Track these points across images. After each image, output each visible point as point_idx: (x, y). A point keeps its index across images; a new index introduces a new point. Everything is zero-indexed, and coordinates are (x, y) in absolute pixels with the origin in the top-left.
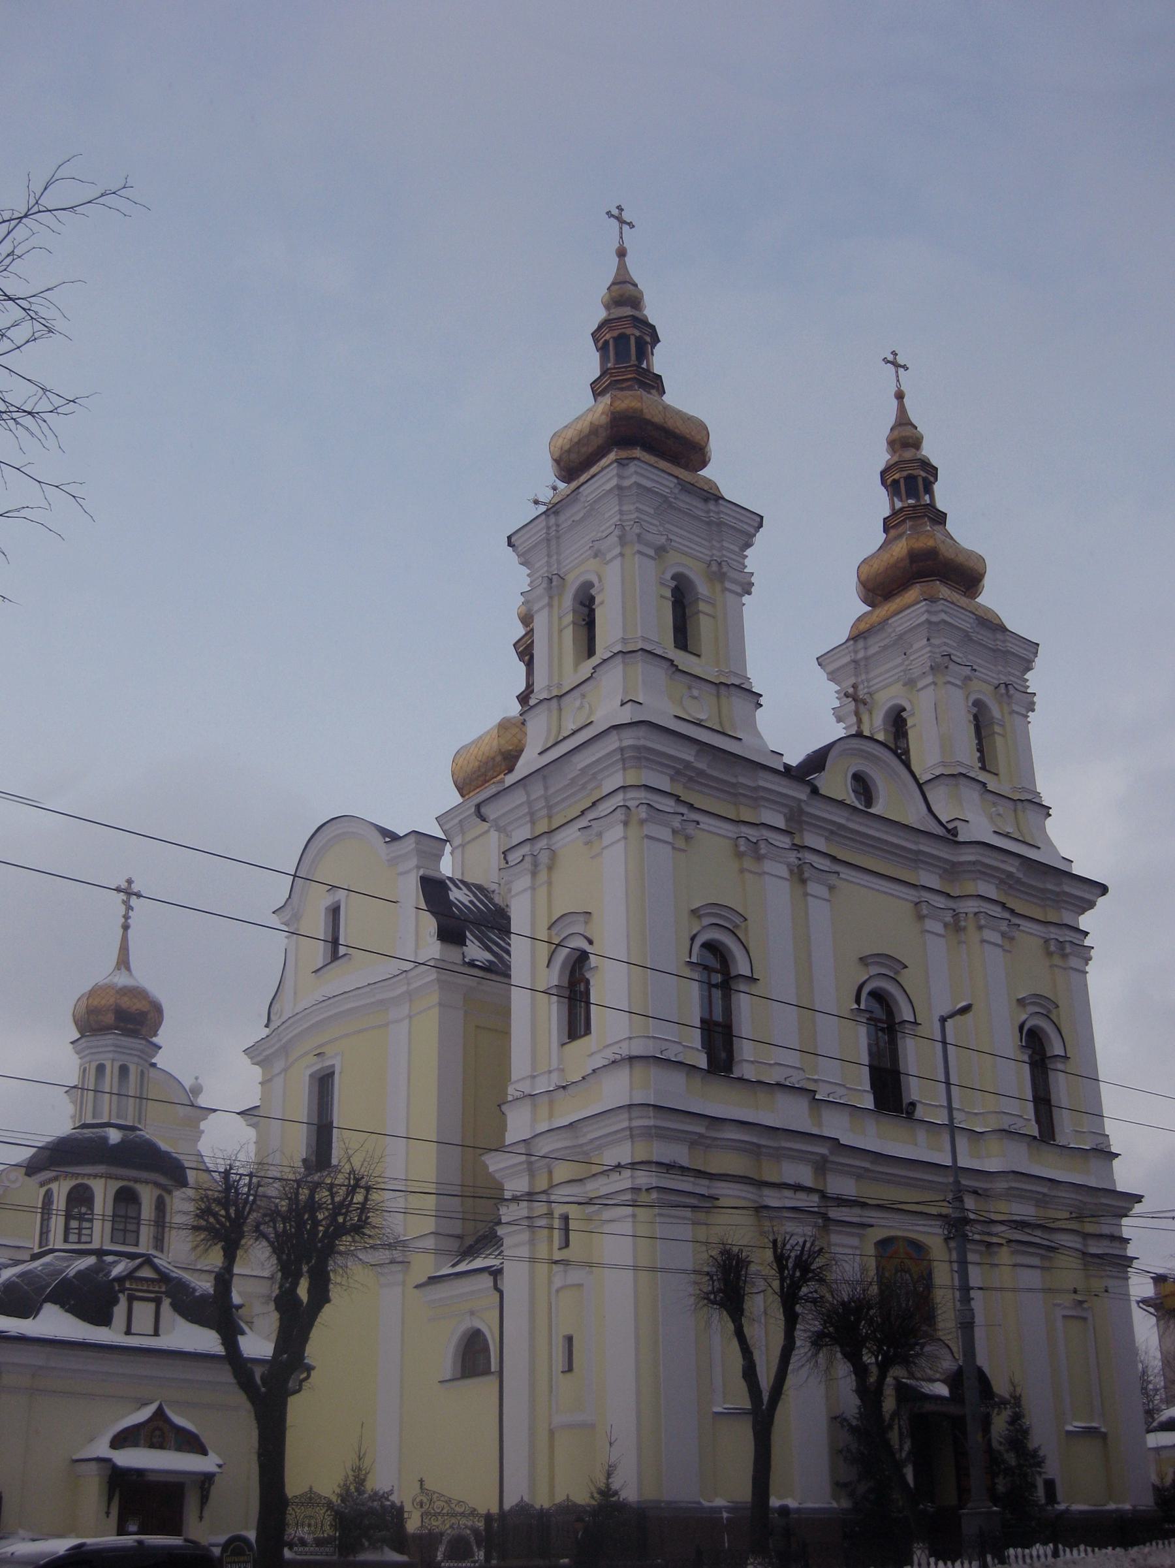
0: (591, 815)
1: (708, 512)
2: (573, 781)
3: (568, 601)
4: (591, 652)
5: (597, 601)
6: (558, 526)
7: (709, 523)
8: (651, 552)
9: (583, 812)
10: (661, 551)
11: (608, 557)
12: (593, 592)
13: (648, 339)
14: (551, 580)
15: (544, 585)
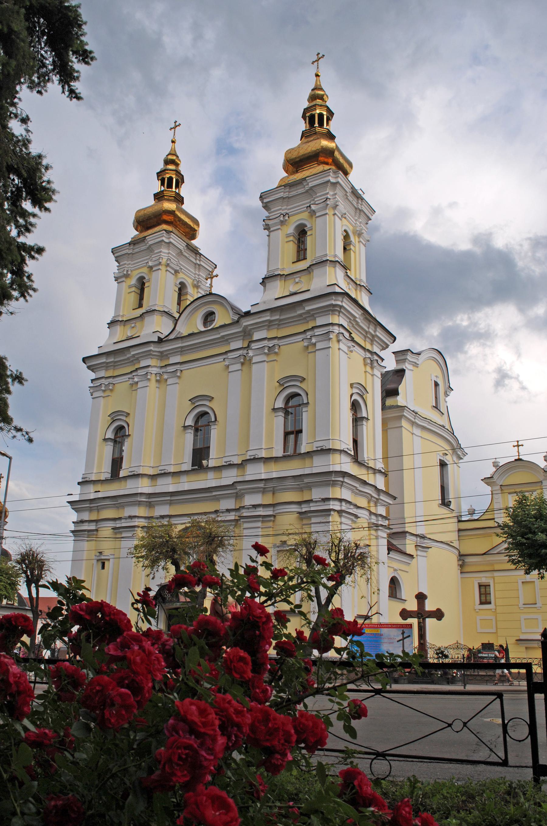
0: (134, 374)
1: (196, 259)
2: (128, 359)
3: (133, 281)
4: (140, 306)
5: (146, 285)
6: (133, 249)
7: (195, 264)
8: (173, 272)
9: (131, 372)
10: (176, 272)
11: (154, 269)
12: (145, 281)
13: (180, 180)
14: (127, 271)
15: (125, 273)
